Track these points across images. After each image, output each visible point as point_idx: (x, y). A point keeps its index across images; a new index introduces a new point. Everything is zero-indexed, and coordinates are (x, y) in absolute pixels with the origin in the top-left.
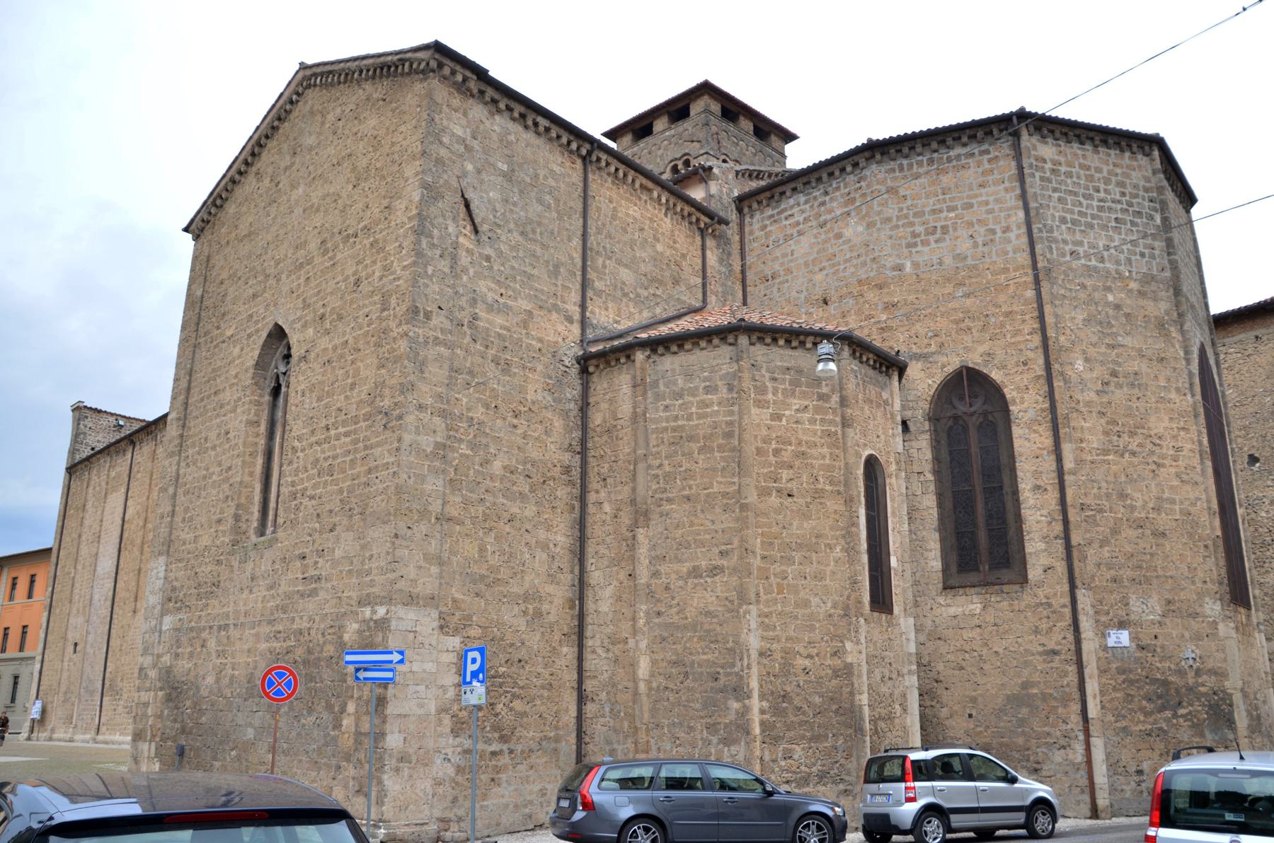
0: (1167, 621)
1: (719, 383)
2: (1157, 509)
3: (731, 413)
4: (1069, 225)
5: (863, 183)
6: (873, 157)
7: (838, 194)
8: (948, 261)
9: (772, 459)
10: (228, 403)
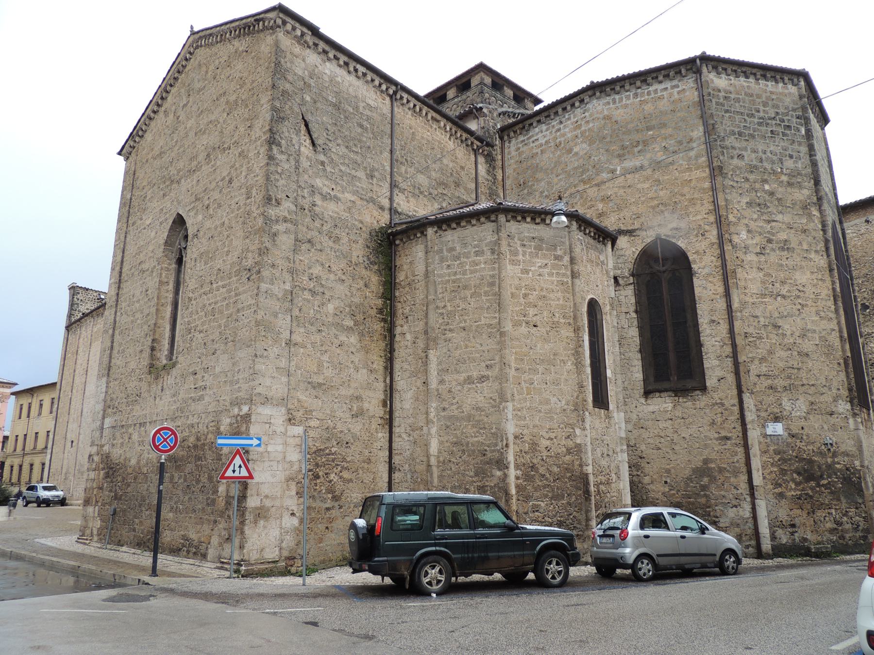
0: (811, 417)
1: (485, 249)
2: (803, 336)
3: (494, 269)
4: (737, 136)
5: (586, 114)
6: (595, 94)
7: (569, 122)
9: (522, 300)
10: (148, 270)
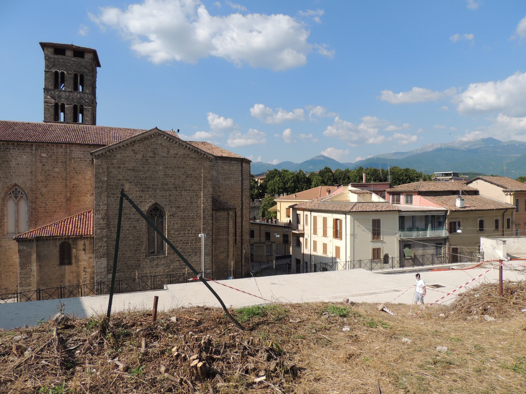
5: (217, 164)
8: (230, 185)
